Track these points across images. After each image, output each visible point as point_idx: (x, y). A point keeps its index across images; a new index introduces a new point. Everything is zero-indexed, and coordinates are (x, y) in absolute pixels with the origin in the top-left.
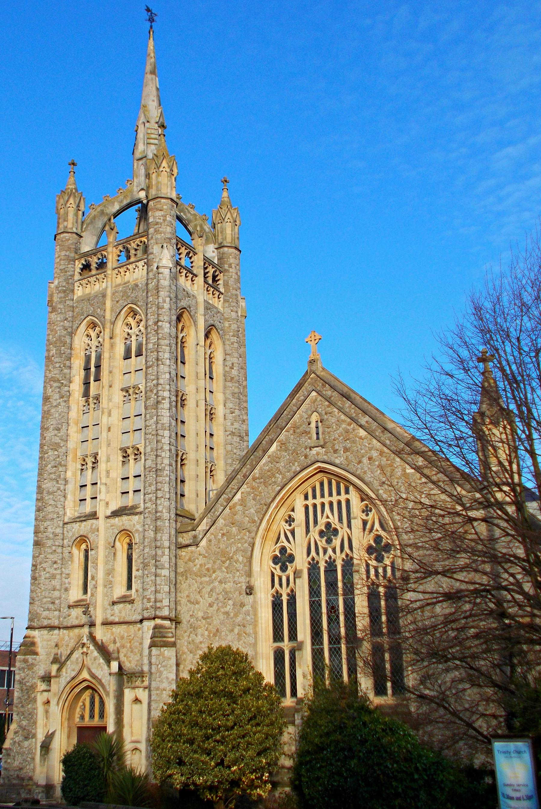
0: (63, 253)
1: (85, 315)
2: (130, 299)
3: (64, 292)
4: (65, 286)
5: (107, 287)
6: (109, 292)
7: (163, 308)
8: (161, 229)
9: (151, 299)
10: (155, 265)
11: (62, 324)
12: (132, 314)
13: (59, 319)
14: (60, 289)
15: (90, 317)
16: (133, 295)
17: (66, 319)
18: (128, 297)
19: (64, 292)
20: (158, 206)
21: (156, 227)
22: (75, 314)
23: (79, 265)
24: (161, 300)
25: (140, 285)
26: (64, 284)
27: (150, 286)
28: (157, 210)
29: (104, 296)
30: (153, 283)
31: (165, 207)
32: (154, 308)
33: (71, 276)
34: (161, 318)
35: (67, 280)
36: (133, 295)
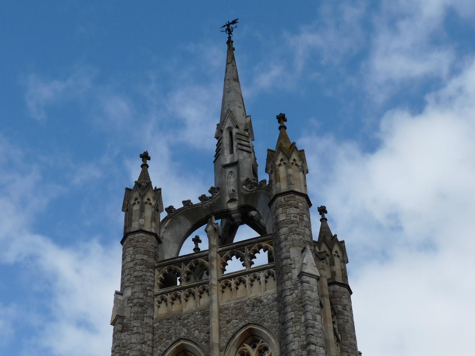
0: (139, 256)
1: (174, 339)
2: (250, 318)
3: (141, 305)
4: (142, 299)
5: (211, 302)
6: (215, 308)
7: (313, 327)
8: (298, 230)
9: (291, 315)
10: (296, 273)
11: (139, 347)
12: (250, 340)
13: (133, 340)
14: (135, 301)
15: (182, 342)
16: (253, 313)
17: (144, 343)
18: (247, 315)
19: (141, 305)
20: (292, 202)
21: (291, 226)
22: (156, 336)
23: (158, 275)
24: (309, 316)
25: (265, 301)
26: (141, 295)
27: (289, 299)
28: (291, 206)
29: (206, 313)
30: (294, 295)
31: (300, 205)
32: (298, 328)
33: (150, 286)
34: (313, 340)
35: (145, 291)
36: (253, 313)
